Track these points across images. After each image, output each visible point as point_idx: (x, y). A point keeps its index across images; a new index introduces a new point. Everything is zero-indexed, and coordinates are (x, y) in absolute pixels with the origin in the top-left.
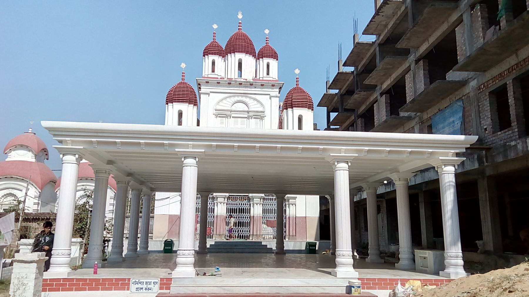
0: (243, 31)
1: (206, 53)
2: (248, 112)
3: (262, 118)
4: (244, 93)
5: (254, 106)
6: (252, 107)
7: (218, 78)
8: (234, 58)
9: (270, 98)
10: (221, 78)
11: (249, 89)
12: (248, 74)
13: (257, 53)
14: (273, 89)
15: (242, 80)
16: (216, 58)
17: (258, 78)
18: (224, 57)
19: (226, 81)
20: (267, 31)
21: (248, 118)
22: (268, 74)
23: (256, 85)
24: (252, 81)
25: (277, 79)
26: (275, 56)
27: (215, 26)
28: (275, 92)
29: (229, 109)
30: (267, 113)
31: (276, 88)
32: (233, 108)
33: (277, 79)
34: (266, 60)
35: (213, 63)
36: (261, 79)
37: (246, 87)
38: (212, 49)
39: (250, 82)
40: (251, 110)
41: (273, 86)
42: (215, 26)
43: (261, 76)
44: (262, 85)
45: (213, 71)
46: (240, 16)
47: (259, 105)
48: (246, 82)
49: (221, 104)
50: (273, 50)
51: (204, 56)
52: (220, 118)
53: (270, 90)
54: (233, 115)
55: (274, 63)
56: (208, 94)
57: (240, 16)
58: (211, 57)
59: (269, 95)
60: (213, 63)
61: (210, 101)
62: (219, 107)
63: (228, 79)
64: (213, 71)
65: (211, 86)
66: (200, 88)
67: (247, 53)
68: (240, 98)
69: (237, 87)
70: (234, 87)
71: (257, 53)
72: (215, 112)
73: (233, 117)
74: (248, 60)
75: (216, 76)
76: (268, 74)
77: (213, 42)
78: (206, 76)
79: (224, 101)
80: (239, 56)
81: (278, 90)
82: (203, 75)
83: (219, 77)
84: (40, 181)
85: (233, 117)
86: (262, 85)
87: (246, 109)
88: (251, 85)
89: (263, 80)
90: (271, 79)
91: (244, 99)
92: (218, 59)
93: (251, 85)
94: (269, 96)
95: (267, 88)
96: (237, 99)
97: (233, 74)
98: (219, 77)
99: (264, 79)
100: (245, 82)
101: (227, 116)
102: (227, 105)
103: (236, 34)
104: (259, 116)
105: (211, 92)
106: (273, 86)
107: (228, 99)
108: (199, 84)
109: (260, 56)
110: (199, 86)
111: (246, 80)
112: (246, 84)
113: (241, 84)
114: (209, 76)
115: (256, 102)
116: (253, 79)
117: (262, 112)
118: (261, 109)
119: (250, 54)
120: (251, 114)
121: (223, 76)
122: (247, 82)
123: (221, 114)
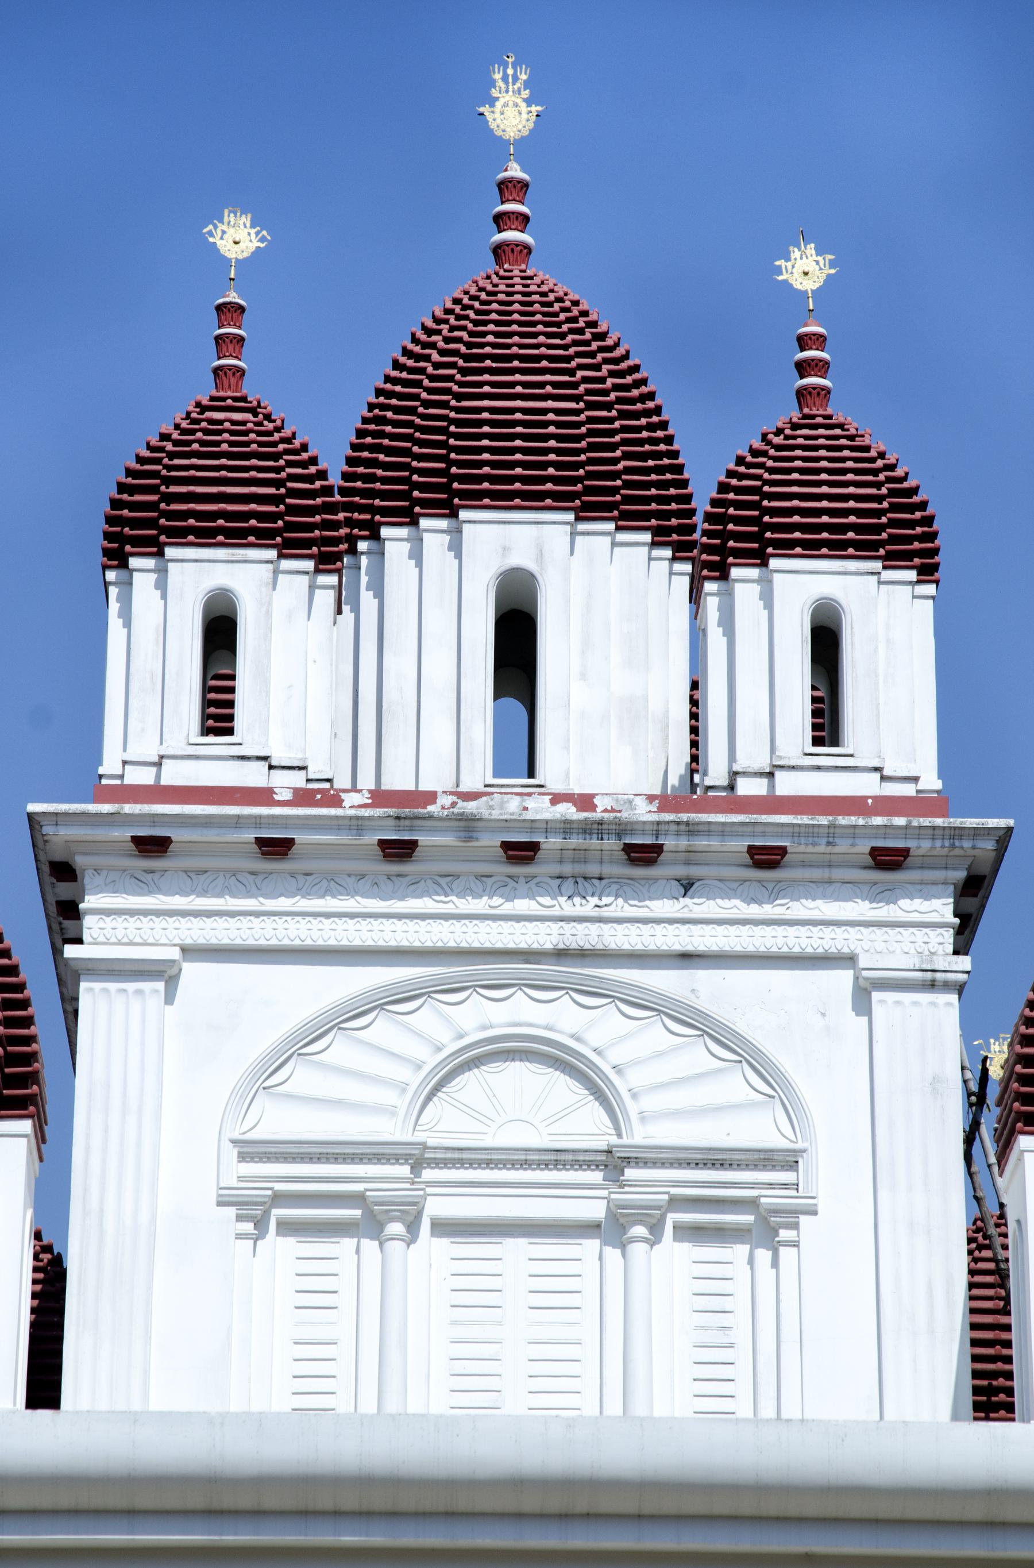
0: (554, 272)
1: (143, 520)
2: (613, 1163)
3: (769, 1229)
4: (561, 955)
5: (679, 1097)
6: (650, 1103)
7: (263, 796)
8: (441, 575)
10: (302, 797)
11: (619, 907)
12: (607, 737)
13: (701, 504)
15: (540, 809)
16: (245, 573)
17: (716, 773)
18: (326, 562)
19: (357, 825)
20: (805, 269)
22: (827, 724)
23: (690, 856)
24: (644, 812)
25: (931, 781)
26: (897, 532)
27: (237, 238)
28: (915, 927)
30: (833, 1176)
31: (924, 890)
32: (447, 1124)
33: (931, 781)
34: (802, 583)
35: (220, 632)
36: (746, 787)
37: (580, 880)
38: (211, 485)
39: (621, 829)
40: (640, 1135)
41: (888, 860)
43: (753, 755)
44: (766, 858)
45: (218, 716)
46: (511, 114)
47: (736, 1085)
48: (587, 829)
49: (300, 1077)
50: (874, 467)
51: (116, 556)
52: (290, 1245)
53: (859, 908)
54: (437, 1207)
55: (890, 618)
56: (164, 973)
57: (511, 114)
58: (196, 574)
59: (849, 960)
60: (220, 632)
62: (277, 1122)
63: (380, 797)
64: (218, 716)
65: (198, 878)
66: (69, 911)
67: (587, 512)
68: (520, 1012)
69: (482, 883)
70: (446, 882)
71: (701, 504)
72: (236, 1172)
73: (444, 1228)
74: (605, 589)
75: (254, 776)
76: (827, 724)
77: (216, 403)
78: (143, 777)
79: (339, 1049)
80: (500, 540)
81: (942, 908)
82: (110, 765)
83: (284, 783)
85: (444, 1228)
86: (766, 858)
87: (587, 1127)
88: (643, 855)
89: (773, 803)
90: (867, 786)
91: (560, 1017)
92: (272, 592)
93: (643, 855)
94: (843, 979)
95: (825, 887)
96: (480, 1015)
97: (440, 739)
98: (284, 783)
99: (787, 785)
100: (567, 828)
101: (371, 1220)
102: (366, 1088)
103: (471, 310)
105: (190, 952)
106: (888, 860)
107: (381, 1029)
108: (63, 871)
109: (723, 539)
110: (64, 890)
111: (585, 802)
112: (581, 856)
113: (521, 852)
114: (174, 775)
115: (699, 1055)
116: (665, 801)
117: (765, 1159)
118: (762, 1130)
119: (628, 519)
120: (648, 1184)
121: (327, 761)
122: (596, 829)
123: (315, 1198)
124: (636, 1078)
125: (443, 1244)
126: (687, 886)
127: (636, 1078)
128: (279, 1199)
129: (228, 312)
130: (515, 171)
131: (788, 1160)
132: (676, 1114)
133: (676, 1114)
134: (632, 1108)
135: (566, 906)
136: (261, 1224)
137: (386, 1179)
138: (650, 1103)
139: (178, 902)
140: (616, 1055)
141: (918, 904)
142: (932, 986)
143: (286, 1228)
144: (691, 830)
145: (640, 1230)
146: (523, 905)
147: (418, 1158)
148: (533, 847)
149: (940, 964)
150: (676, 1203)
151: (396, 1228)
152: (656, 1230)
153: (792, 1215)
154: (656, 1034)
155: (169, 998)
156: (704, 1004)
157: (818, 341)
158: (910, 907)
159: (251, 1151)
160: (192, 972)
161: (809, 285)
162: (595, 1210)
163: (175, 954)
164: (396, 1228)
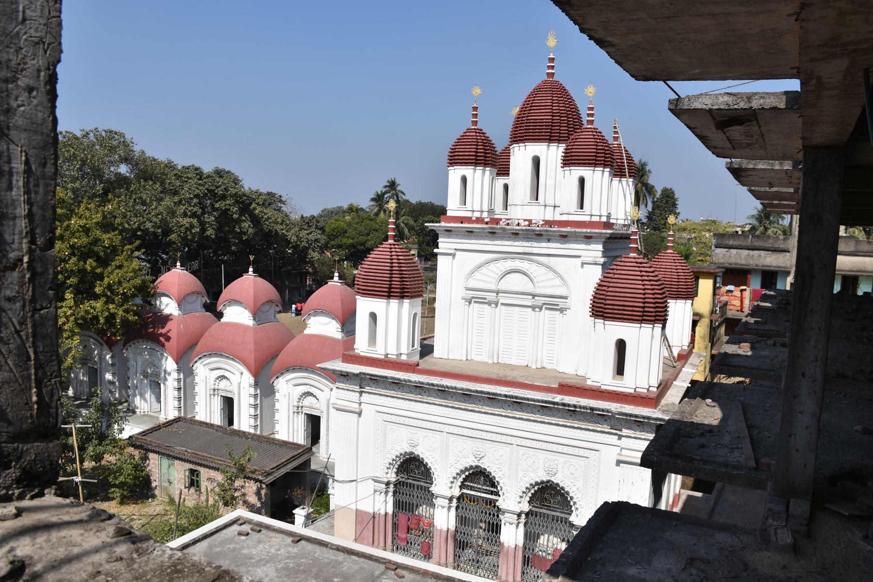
2: (534, 296)
3: (562, 310)
5: (546, 284)
6: (540, 284)
9: (582, 267)
11: (535, 244)
14: (588, 244)
16: (467, 171)
21: (533, 308)
23: (549, 235)
27: (477, 91)
29: (492, 287)
32: (504, 285)
42: (477, 91)
47: (558, 281)
49: (477, 275)
53: (583, 246)
54: (502, 301)
59: (579, 257)
61: (457, 266)
70: (502, 238)
73: (502, 304)
79: (484, 270)
81: (600, 247)
84: (252, 362)
85: (502, 304)
87: (529, 287)
90: (587, 219)
94: (578, 261)
102: (487, 279)
104: (555, 304)
107: (492, 266)
112: (527, 234)
115: (551, 275)
120: (540, 301)
124: (538, 279)
125: (503, 307)
126: (549, 241)
127: (538, 279)
128: (473, 298)
129: (475, 109)
130: (552, 56)
131: (566, 298)
132: (545, 287)
133: (545, 287)
134: (537, 285)
135: (525, 244)
136: (470, 303)
137: (491, 296)
138: (540, 284)
139: (454, 240)
140: (534, 274)
141: (595, 246)
142: (596, 264)
143: (475, 302)
144: (547, 231)
145: (537, 309)
146: (517, 243)
147: (498, 292)
148: (517, 234)
149: (597, 260)
150: (544, 304)
151: (493, 305)
152: (541, 309)
153: (566, 309)
154: (543, 270)
155: (454, 258)
156: (551, 265)
157: (592, 109)
158: (593, 246)
159: (468, 289)
160: (458, 253)
161: (591, 95)
162: (529, 304)
163: (452, 252)
164: (493, 305)
